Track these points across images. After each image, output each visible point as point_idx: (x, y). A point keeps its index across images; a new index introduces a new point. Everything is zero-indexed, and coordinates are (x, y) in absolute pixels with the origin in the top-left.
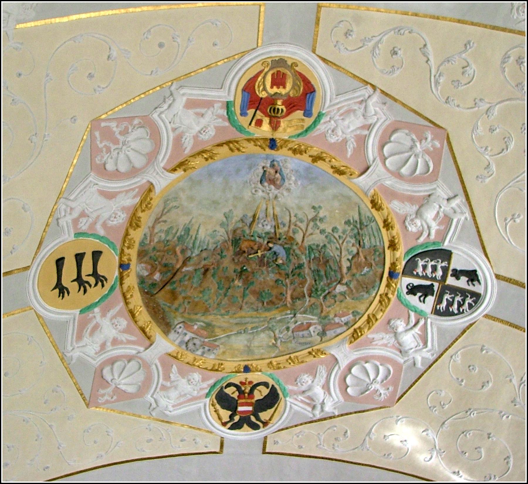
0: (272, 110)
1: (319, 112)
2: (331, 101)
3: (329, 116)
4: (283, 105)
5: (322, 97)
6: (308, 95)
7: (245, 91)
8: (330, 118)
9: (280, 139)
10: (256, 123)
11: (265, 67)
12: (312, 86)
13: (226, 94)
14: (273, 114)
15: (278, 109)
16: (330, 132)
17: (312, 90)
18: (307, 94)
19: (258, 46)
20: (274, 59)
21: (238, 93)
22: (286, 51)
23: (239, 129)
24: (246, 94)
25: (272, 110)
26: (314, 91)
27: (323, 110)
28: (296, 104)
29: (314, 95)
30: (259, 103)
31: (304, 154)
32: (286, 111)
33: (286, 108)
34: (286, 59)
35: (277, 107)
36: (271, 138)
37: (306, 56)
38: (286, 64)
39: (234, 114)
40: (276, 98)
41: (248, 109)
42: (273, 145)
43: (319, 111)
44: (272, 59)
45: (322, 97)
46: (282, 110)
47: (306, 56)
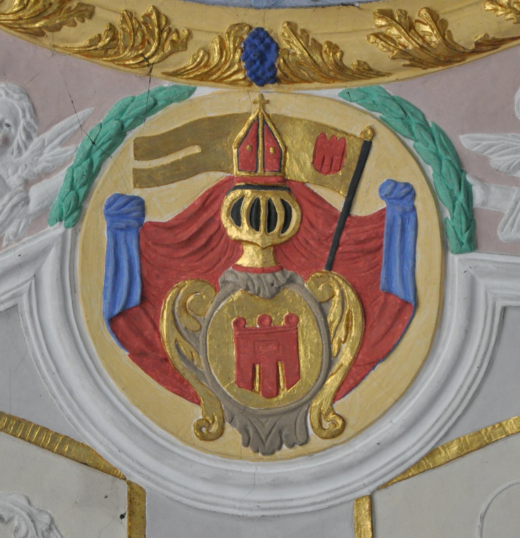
0: (280, 222)
1: (78, 221)
2: (37, 279)
3: (33, 207)
4: (239, 242)
5: (74, 291)
6: (136, 297)
7: (405, 303)
8: (26, 201)
9: (234, 83)
10: (343, 154)
11: (331, 409)
12: (123, 343)
13: (482, 284)
14: (270, 194)
15: (255, 224)
16: (20, 137)
17: (121, 321)
18: (143, 298)
19: (371, 497)
20: (298, 449)
21: (435, 289)
22: (253, 486)
23: (413, 122)
24: (397, 287)
25: (280, 222)
26: (112, 321)
27: (64, 236)
28: (184, 253)
29: (113, 304)
30: (337, 244)
31: (117, 20)
32: (218, 213)
33: (221, 230)
34: (249, 451)
35: (257, 237)
36: (271, 87)
37: (166, 471)
38: (244, 431)
39: (442, 192)
40: (269, 277)
41: (381, 215)
42: (262, 58)
43: (84, 226)
44: (309, 447)
45: (74, 291)
46: (238, 223)
47: (166, 471)
